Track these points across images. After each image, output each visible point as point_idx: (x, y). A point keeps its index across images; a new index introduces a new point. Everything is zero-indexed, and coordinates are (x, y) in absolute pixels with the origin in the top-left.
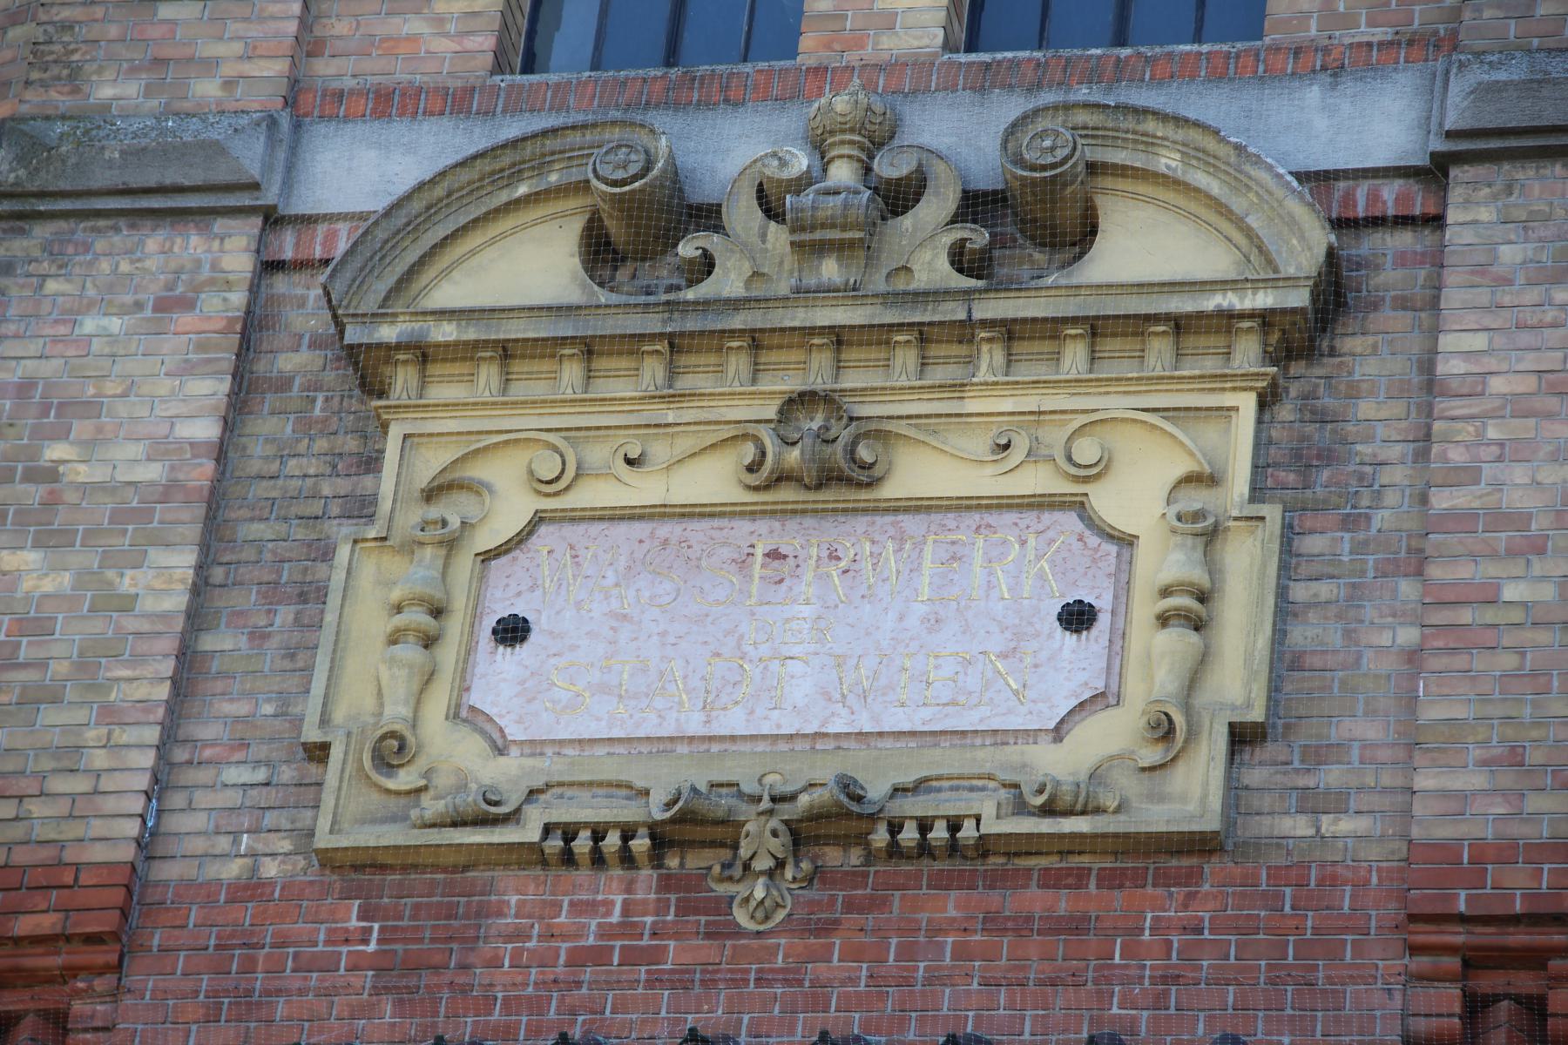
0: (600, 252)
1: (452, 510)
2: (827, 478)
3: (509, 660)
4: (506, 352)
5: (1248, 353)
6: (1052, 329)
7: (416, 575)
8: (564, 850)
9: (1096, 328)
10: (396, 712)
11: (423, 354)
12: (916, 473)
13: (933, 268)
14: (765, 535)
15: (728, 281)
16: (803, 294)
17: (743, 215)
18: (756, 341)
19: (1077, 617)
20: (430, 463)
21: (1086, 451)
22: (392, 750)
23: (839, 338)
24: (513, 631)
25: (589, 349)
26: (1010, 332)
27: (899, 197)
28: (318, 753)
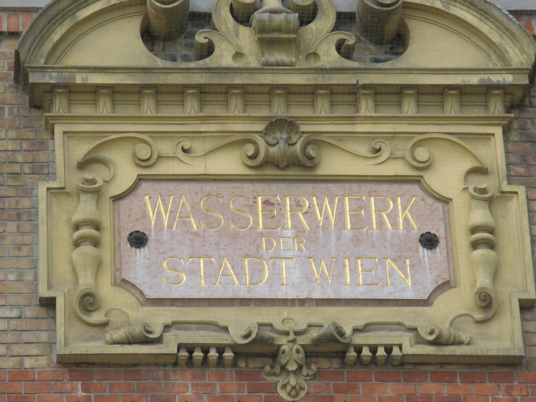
0: (148, 36)
1: (98, 174)
2: (293, 163)
3: (141, 255)
4: (114, 91)
5: (497, 107)
6: (400, 91)
7: (85, 209)
8: (192, 359)
9: (420, 91)
10: (86, 281)
11: (71, 91)
12: (333, 164)
13: (329, 56)
14: (260, 193)
15: (223, 56)
16: (268, 67)
17: (224, 19)
18: (246, 91)
19: (429, 241)
20: (81, 150)
21: (422, 154)
22: (88, 301)
23: (289, 91)
24: (138, 240)
25: (159, 91)
26: (378, 92)
27: (308, 15)
28: (49, 304)
